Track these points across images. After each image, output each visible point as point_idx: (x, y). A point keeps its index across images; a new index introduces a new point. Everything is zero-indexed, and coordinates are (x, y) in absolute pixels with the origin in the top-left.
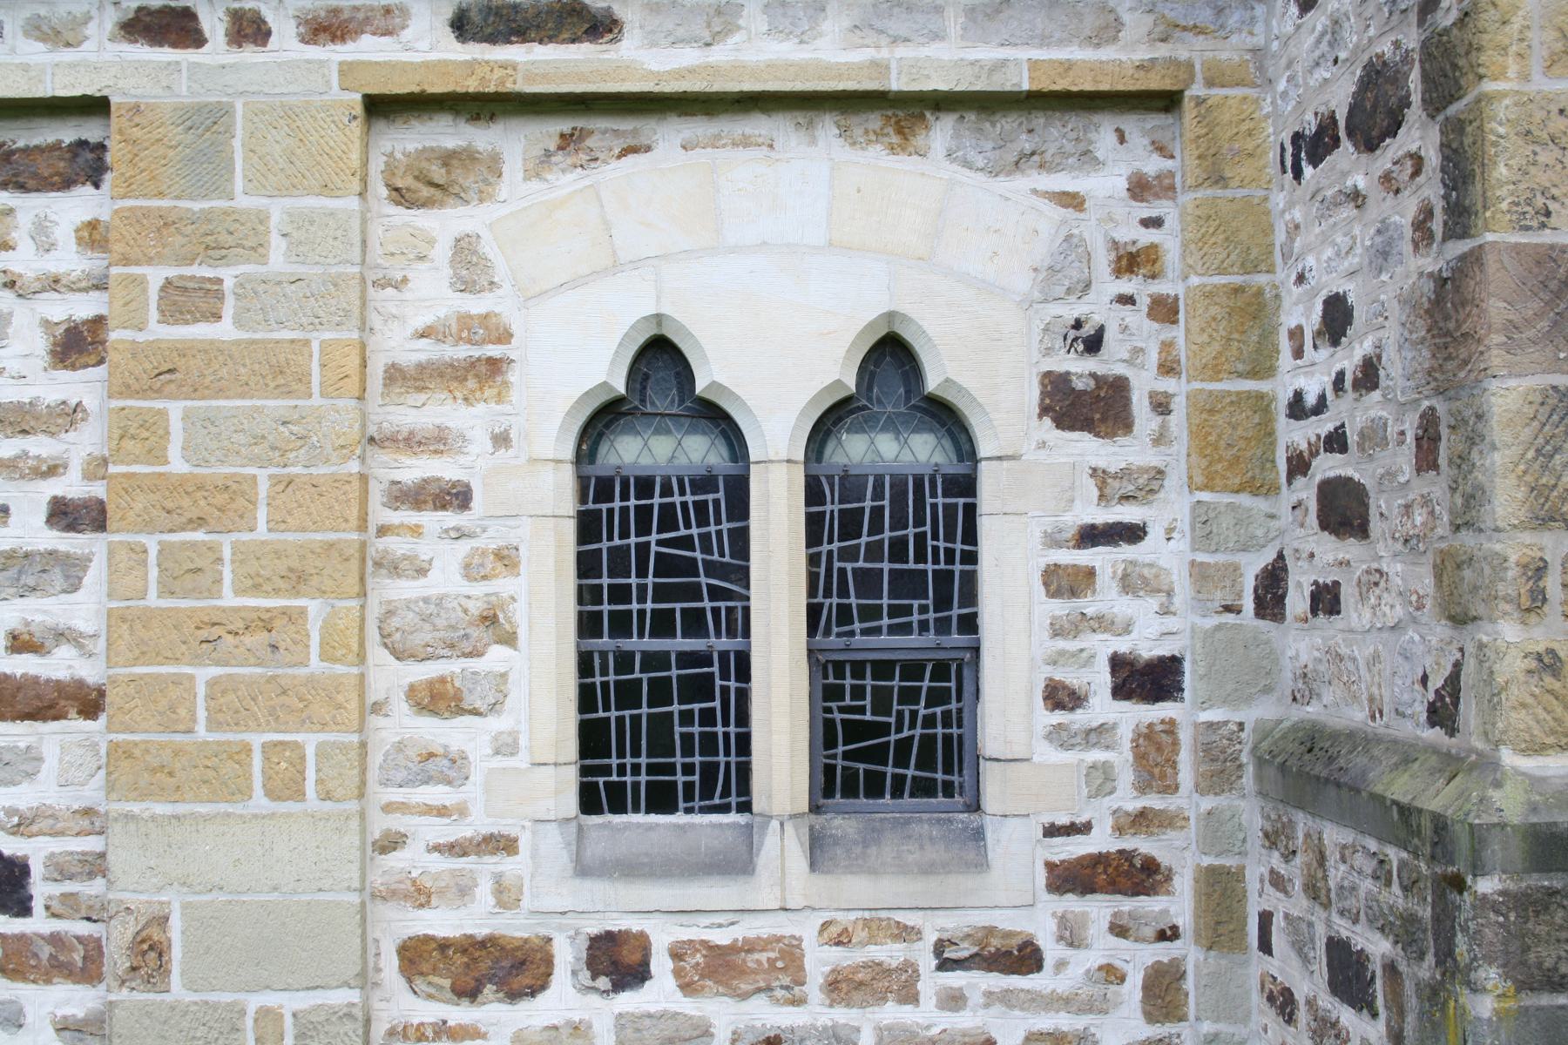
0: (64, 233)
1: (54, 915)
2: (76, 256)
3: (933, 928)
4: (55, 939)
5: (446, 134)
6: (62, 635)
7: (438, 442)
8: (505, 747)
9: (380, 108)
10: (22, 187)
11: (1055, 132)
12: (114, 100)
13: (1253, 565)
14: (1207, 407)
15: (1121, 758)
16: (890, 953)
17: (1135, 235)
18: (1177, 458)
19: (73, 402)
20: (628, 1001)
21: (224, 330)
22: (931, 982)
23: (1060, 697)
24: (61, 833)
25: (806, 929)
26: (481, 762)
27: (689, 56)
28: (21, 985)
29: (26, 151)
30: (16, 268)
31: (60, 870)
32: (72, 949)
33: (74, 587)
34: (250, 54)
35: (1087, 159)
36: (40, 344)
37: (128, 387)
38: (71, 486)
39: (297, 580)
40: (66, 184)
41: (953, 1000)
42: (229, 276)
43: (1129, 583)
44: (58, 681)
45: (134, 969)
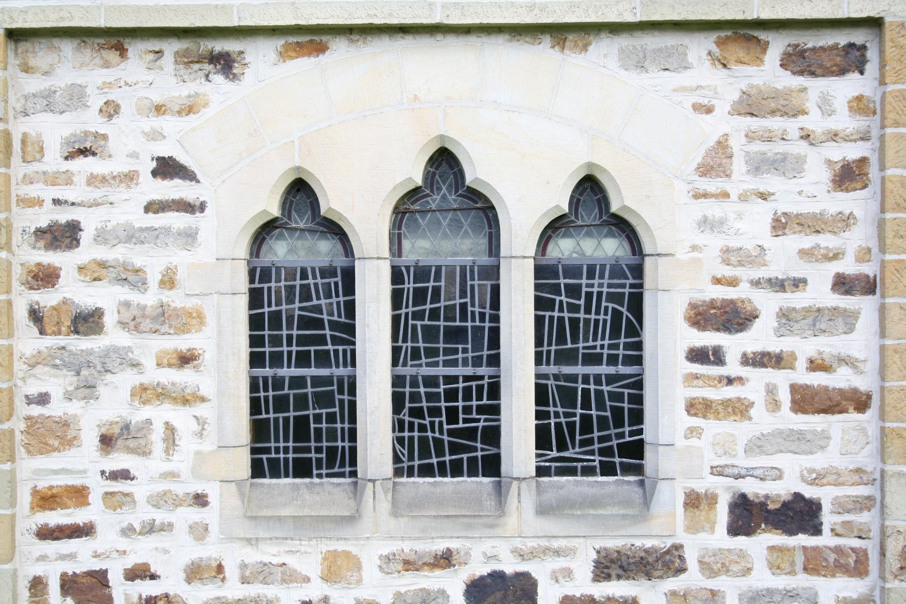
0: (841, 104)
1: (837, 535)
2: (848, 119)
4: (838, 550)
6: (844, 361)
10: (813, 74)
12: (888, 20)
19: (847, 212)
24: (843, 484)
28: (815, 578)
29: (814, 49)
30: (810, 126)
31: (841, 507)
32: (848, 556)
33: (850, 329)
36: (825, 176)
37: (898, 205)
38: (848, 266)
40: (842, 72)
44: (840, 389)
45: (902, 568)
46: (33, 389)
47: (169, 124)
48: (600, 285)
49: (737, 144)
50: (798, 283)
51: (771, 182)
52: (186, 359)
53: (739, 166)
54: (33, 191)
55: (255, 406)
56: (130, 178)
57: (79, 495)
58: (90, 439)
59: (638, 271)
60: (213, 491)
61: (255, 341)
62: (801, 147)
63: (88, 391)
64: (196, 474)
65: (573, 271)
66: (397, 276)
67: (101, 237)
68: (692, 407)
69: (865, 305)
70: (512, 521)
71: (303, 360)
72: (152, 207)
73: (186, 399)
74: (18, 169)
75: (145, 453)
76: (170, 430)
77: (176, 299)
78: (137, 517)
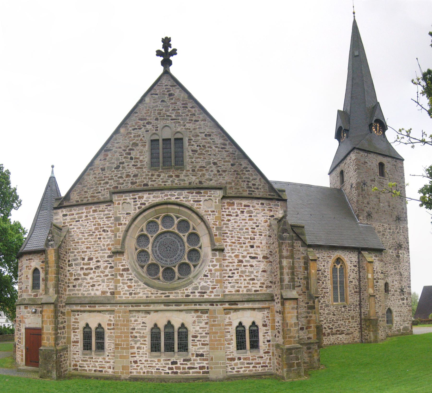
3: (257, 356)
5: (228, 311)
7: (228, 329)
8: (233, 346)
9: (224, 309)
11: (263, 310)
13: (274, 334)
14: (272, 325)
15: (267, 346)
16: (255, 357)
17: (267, 315)
18: (270, 328)
20: (240, 361)
21: (216, 323)
22: (257, 359)
23: (264, 342)
25: (250, 356)
26: (231, 347)
27: (242, 306)
31: (206, 354)
34: (217, 307)
35: (265, 311)
38: (206, 332)
39: (221, 337)
41: (258, 360)
42: (216, 320)
43: (268, 335)
46: (131, 343)
47: (143, 319)
48: (184, 334)
49: (196, 320)
50: (202, 333)
51: (200, 324)
52: (145, 341)
53: (196, 322)
54: (131, 325)
55: (151, 345)
56: (140, 324)
57: (135, 353)
58: (136, 348)
59: (187, 332)
60: (147, 353)
61: (151, 339)
62: (202, 321)
63: (136, 343)
64: (146, 351)
65: (181, 332)
66: (165, 333)
67: (137, 329)
68: (193, 345)
69: (208, 335)
70: (175, 356)
71: (156, 341)
72: (142, 326)
73: (145, 344)
74: (130, 323)
75: (141, 349)
76: (143, 347)
77: (144, 335)
78: (141, 355)
